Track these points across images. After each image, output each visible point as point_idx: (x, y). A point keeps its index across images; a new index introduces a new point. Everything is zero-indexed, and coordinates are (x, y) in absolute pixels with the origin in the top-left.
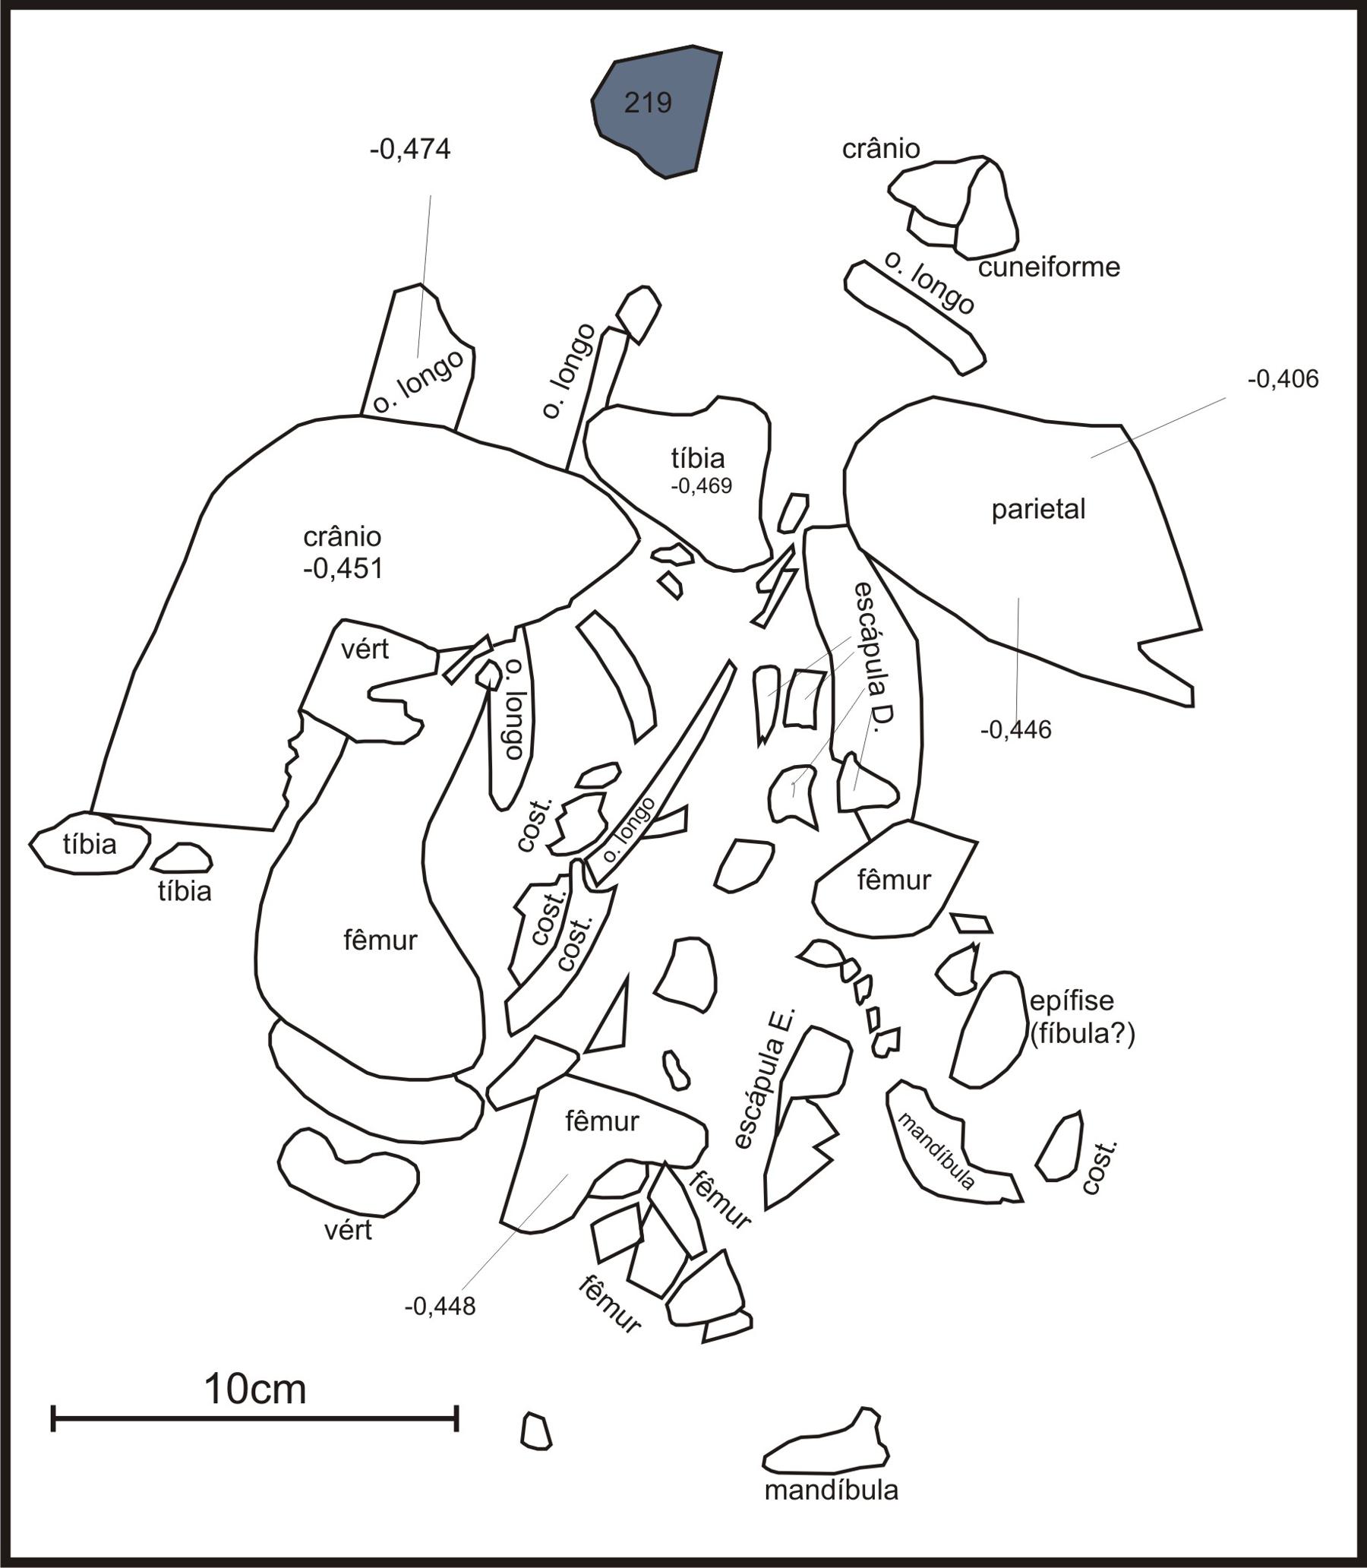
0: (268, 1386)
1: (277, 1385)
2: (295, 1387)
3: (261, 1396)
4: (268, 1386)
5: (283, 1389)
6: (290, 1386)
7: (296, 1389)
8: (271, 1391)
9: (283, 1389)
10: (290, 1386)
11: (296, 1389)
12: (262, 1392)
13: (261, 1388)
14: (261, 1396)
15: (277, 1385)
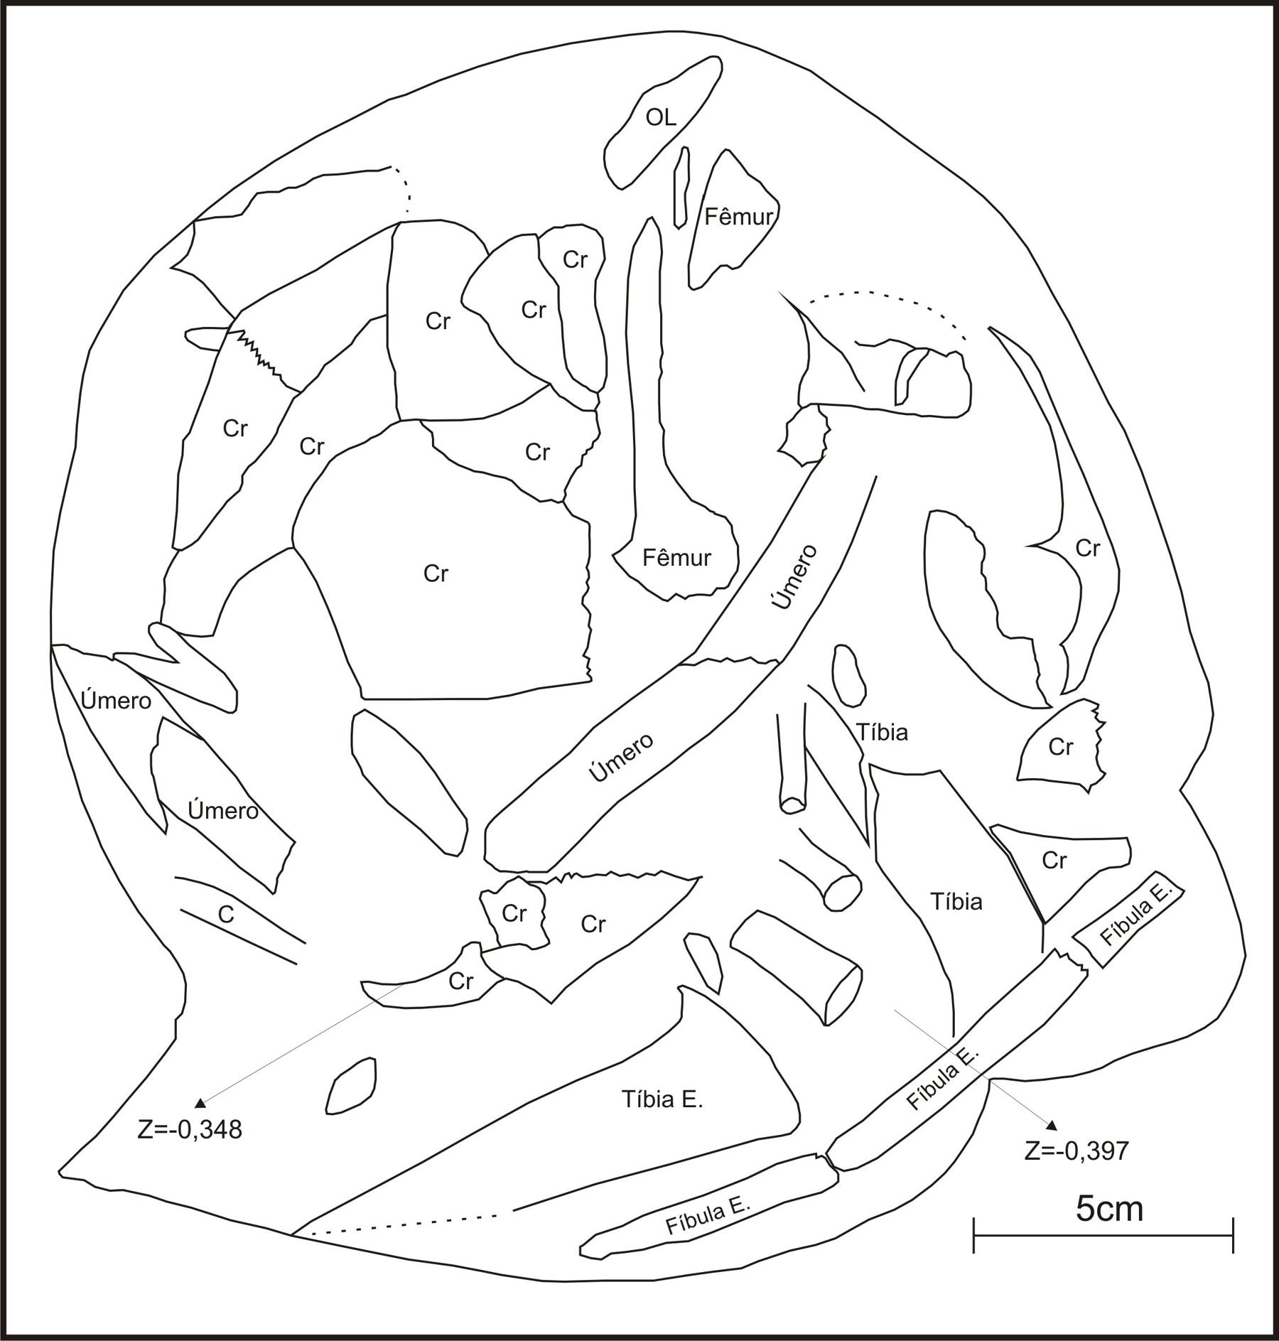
0: (1111, 1206)
1: (1119, 1205)
2: (1133, 1208)
3: (1105, 1215)
4: (1111, 1206)
5: (1124, 1208)
6: (1129, 1206)
7: (1135, 1209)
8: (1114, 1211)
9: (1124, 1208)
10: (1129, 1206)
11: (1135, 1209)
12: (1106, 1211)
13: (1105, 1207)
14: (1105, 1215)
15: (1119, 1205)
